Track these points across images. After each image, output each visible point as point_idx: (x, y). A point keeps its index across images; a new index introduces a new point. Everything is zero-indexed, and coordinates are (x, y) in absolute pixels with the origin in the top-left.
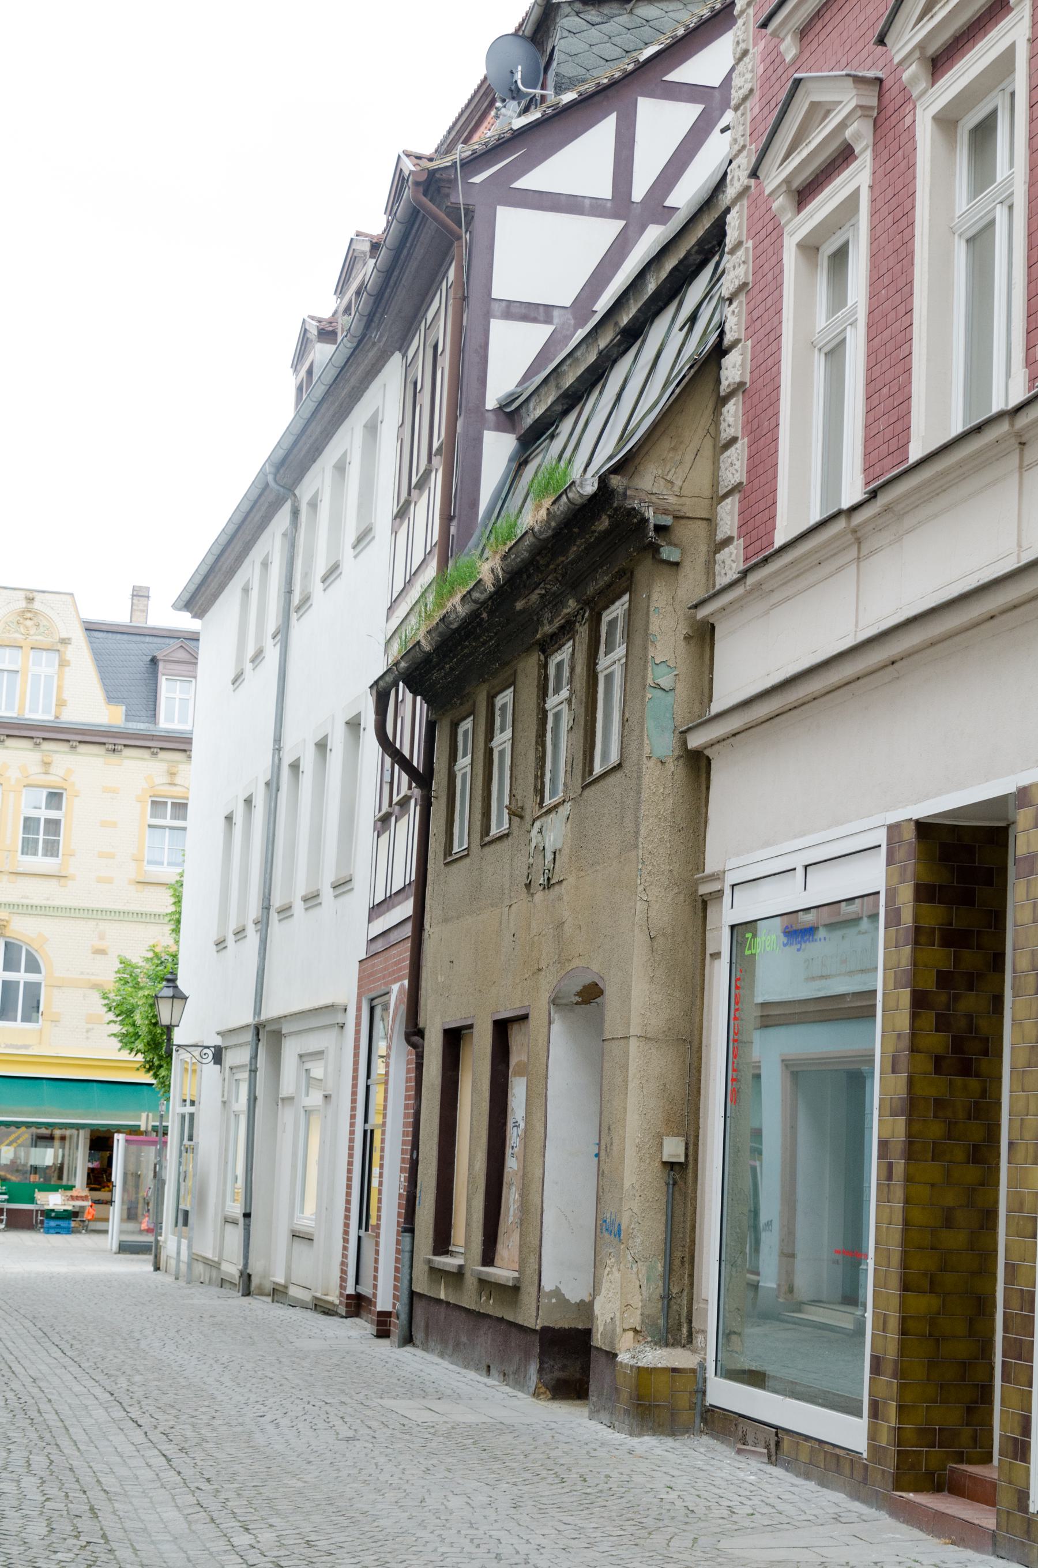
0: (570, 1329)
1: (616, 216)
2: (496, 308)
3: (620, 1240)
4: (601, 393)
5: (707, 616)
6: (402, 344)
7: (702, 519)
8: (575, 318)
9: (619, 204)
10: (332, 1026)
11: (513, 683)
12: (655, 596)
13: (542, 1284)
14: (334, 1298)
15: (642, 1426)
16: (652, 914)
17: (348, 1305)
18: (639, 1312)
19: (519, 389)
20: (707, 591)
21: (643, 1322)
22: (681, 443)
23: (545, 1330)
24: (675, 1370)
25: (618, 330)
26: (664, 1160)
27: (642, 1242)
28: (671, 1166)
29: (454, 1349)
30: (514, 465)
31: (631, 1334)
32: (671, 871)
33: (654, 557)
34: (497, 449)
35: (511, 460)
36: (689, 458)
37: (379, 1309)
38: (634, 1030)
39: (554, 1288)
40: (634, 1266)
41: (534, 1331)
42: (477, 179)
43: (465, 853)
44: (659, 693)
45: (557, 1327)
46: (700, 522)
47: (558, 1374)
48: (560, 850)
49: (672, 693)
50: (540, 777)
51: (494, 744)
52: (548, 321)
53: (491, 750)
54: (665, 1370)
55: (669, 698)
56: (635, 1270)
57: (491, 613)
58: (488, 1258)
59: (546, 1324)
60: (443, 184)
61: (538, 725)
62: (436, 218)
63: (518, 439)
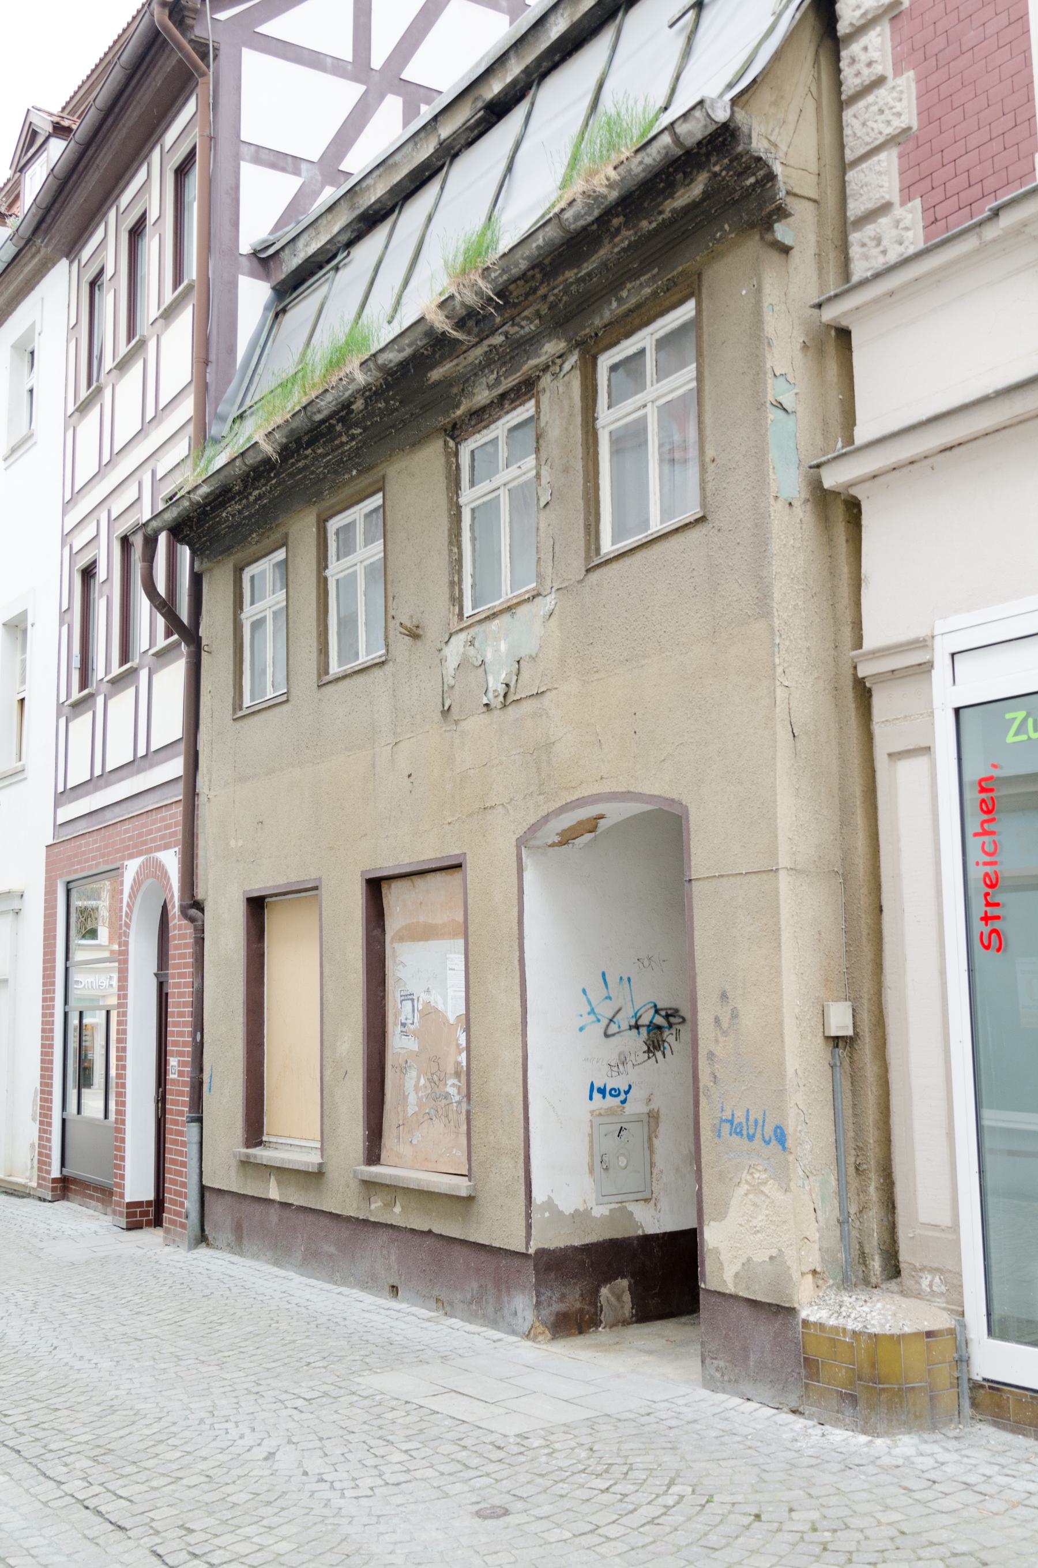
0: (567, 1248)
1: (356, 79)
2: (245, 150)
3: (784, 1148)
4: (442, 188)
5: (838, 317)
6: (71, 249)
7: (809, 199)
8: (322, 174)
9: (358, 67)
10: (6, 912)
11: (382, 489)
12: (767, 289)
13: (534, 1195)
14: (26, 1176)
15: (890, 1420)
16: (794, 704)
17: (53, 1189)
18: (817, 1246)
19: (271, 238)
20: (821, 293)
21: (823, 1259)
22: (782, 97)
23: (541, 1252)
24: (929, 1334)
25: (480, 104)
26: (833, 1033)
27: (812, 1149)
28: (836, 1041)
29: (240, 1240)
30: (271, 315)
31: (810, 1276)
32: (808, 649)
33: (762, 238)
34: (253, 295)
35: (267, 309)
36: (792, 117)
37: (127, 1199)
38: (784, 861)
39: (545, 1199)
40: (806, 1183)
41: (525, 1256)
42: (223, 16)
43: (284, 698)
44: (781, 413)
45: (552, 1247)
46: (806, 203)
47: (557, 1307)
48: (533, 658)
49: (792, 416)
50: (455, 584)
51: (328, 573)
52: (297, 172)
53: (326, 579)
54: (917, 1334)
55: (789, 422)
56: (807, 1188)
57: (368, 401)
58: (373, 1156)
59: (541, 1246)
60: (186, 13)
61: (451, 523)
62: (181, 49)
63: (273, 288)
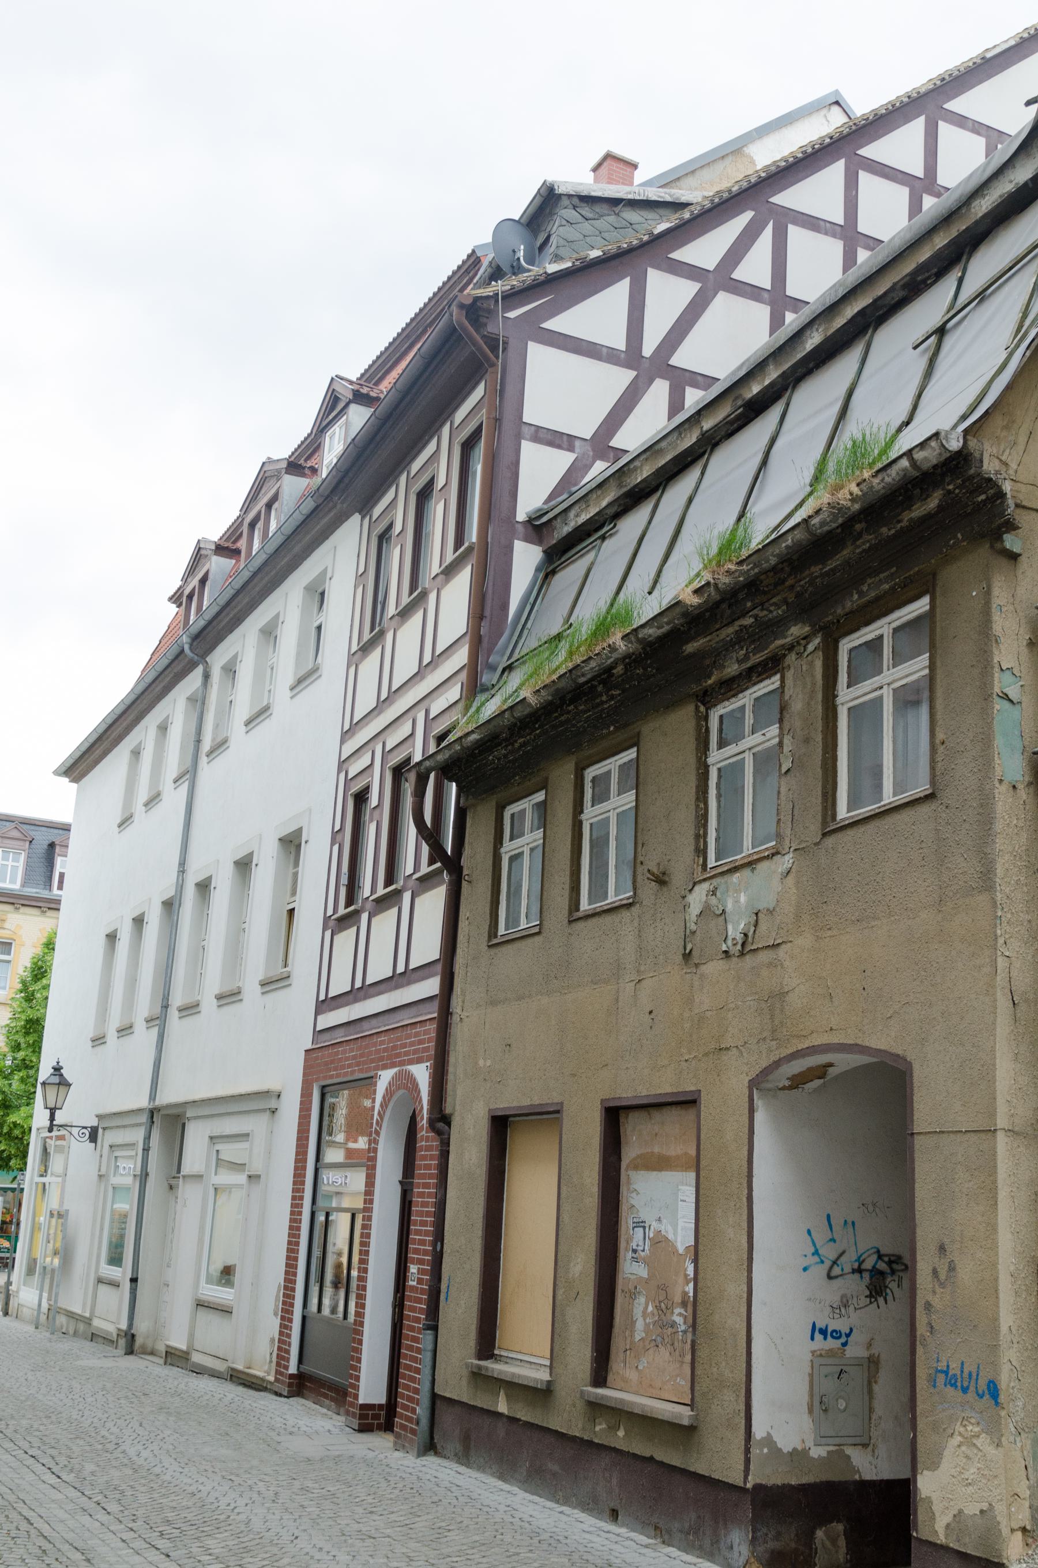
1: (628, 366)
2: (525, 430)
3: (997, 1403)
4: (703, 474)
6: (365, 507)
8: (593, 450)
9: (630, 356)
10: (264, 1110)
11: (636, 744)
12: (996, 591)
13: (754, 1429)
14: (263, 1369)
16: (1014, 974)
17: (290, 1385)
18: (1027, 1504)
19: (546, 507)
22: (1013, 422)
23: (758, 1487)
25: (740, 403)
29: (465, 1454)
30: (541, 575)
31: (1019, 1534)
32: (1029, 921)
33: (992, 547)
34: (526, 559)
35: (538, 570)
36: (1022, 439)
37: (361, 1401)
38: (1002, 1122)
39: (764, 1435)
40: (1018, 1439)
41: (743, 1490)
42: (512, 315)
43: (536, 930)
44: (1006, 704)
47: (771, 1545)
48: (771, 912)
49: (1018, 707)
50: (701, 836)
51: (583, 817)
52: (571, 449)
53: (581, 823)
55: (1015, 712)
56: (1019, 1445)
58: (600, 1376)
59: (758, 1481)
60: (481, 313)
62: (475, 343)
63: (544, 552)
